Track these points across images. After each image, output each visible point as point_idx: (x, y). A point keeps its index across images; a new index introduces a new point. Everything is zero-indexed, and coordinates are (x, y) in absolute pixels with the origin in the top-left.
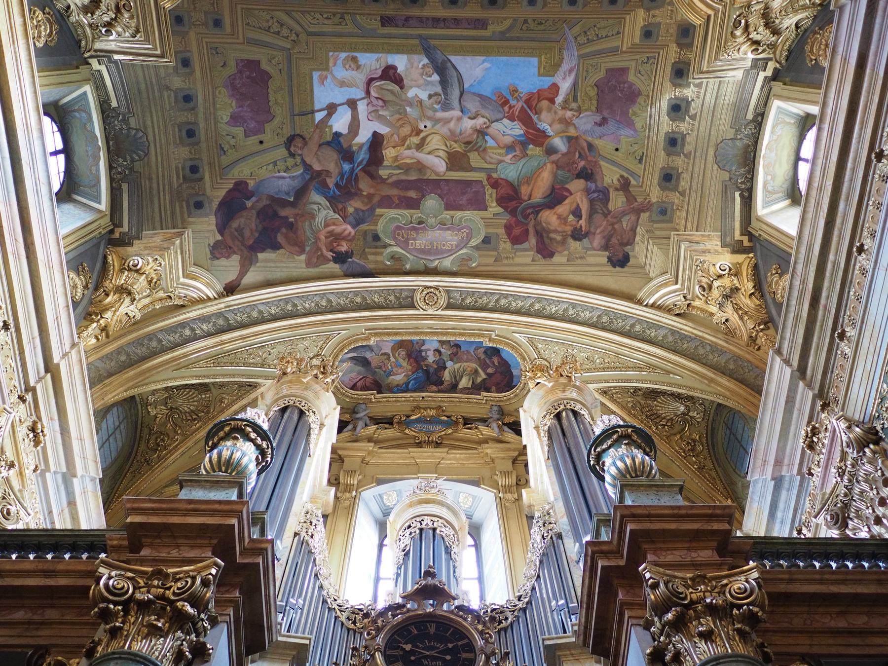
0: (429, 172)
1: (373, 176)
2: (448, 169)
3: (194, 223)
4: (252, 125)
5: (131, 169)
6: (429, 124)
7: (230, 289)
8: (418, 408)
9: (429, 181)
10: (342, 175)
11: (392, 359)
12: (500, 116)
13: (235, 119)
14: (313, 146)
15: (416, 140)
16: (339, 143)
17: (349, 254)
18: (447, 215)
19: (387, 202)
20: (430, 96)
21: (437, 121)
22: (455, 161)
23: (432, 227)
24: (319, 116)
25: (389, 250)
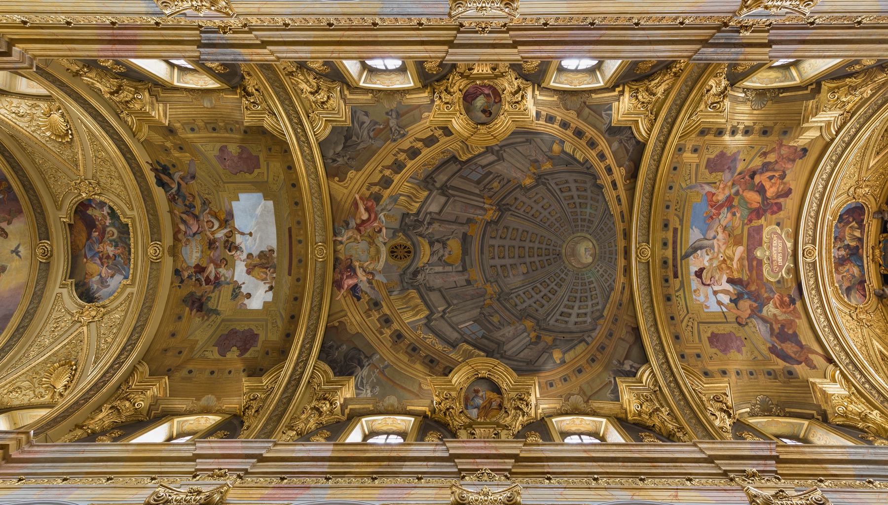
0: (744, 255)
1: (748, 284)
2: (742, 245)
3: (802, 376)
4: (739, 343)
5: (777, 405)
6: (721, 255)
7: (830, 360)
8: (873, 260)
9: (748, 255)
10: (750, 299)
11: (845, 274)
12: (717, 220)
13: (739, 351)
14: (739, 313)
15: (728, 262)
16: (735, 300)
17: (790, 296)
18: (765, 246)
20: (708, 255)
21: (719, 251)
22: (738, 242)
23: (771, 253)
24: (725, 310)
25: (784, 275)
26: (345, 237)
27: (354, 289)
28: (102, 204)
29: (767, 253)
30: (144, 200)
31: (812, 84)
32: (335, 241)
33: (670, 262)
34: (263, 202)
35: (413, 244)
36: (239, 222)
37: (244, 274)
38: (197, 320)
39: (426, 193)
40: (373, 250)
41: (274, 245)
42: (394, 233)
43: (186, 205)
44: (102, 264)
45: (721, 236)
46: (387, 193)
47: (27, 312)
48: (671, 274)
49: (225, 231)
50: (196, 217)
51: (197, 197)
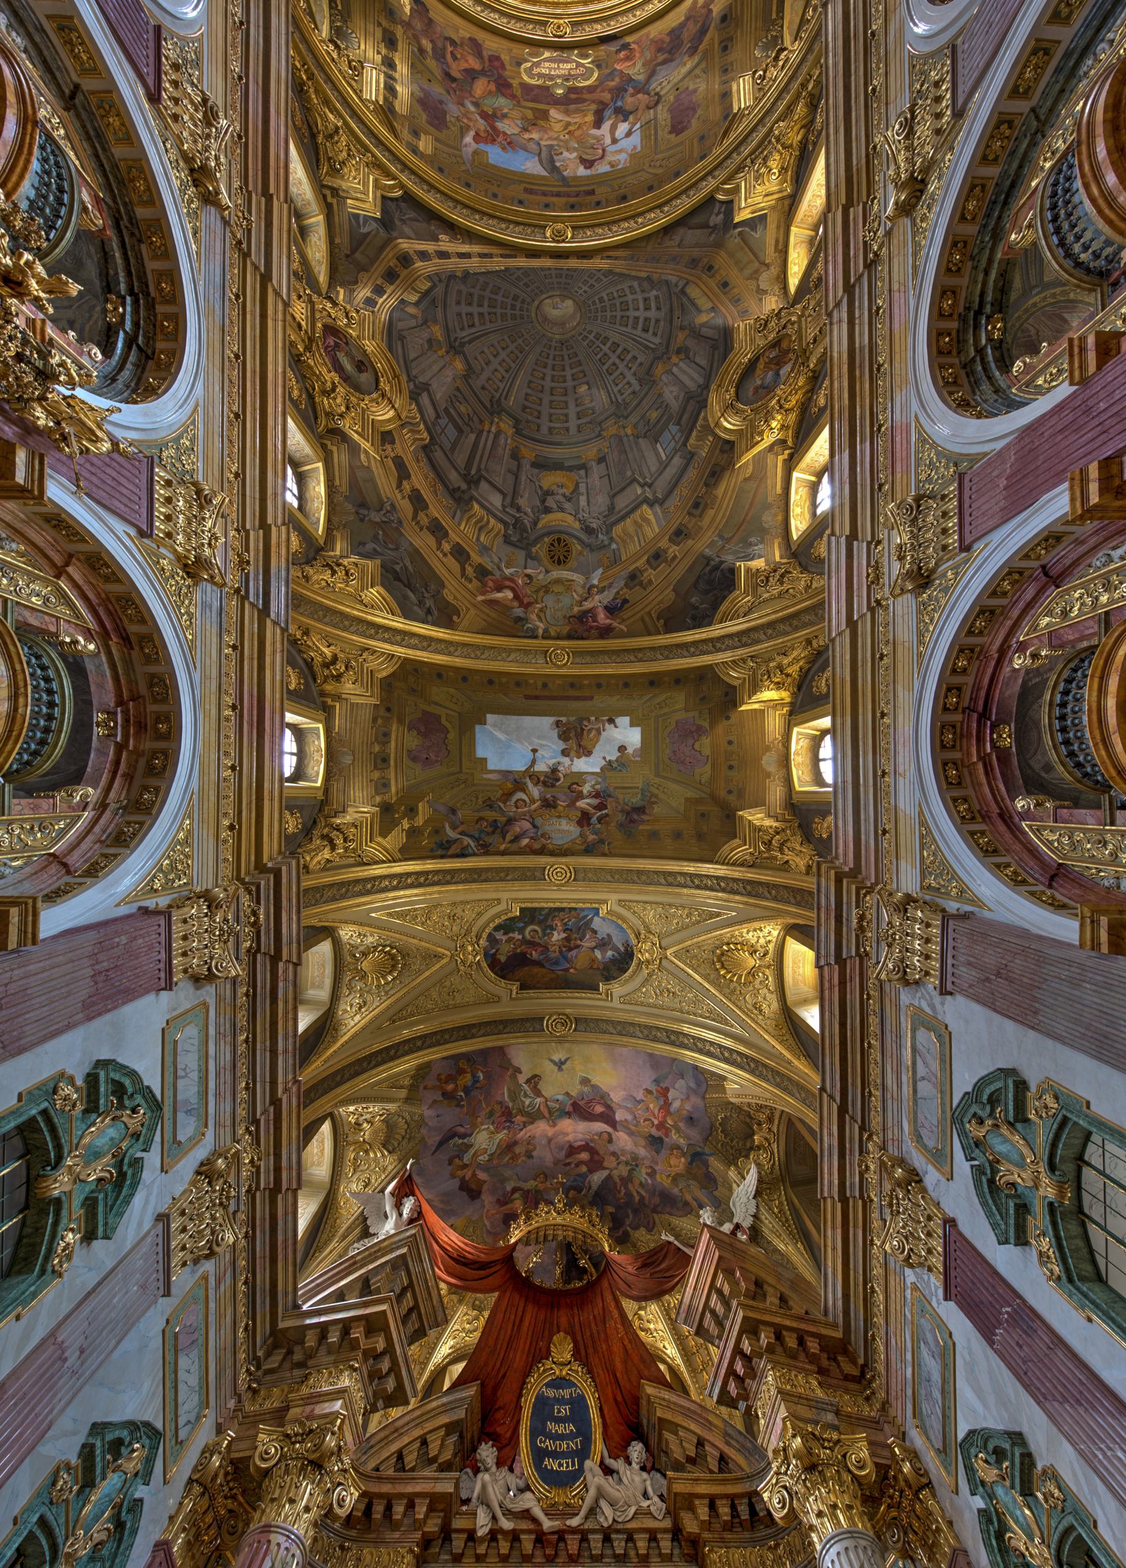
15: (571, 128)
19: (591, 89)
22: (545, 115)
23: (559, 76)
26: (538, 623)
27: (608, 609)
28: (491, 938)
29: (559, 81)
30: (485, 881)
31: (325, 197)
32: (544, 638)
33: (572, 200)
34: (487, 727)
35: (548, 534)
36: (518, 764)
37: (591, 759)
38: (656, 810)
39: (476, 506)
40: (557, 588)
41: (550, 720)
42: (532, 558)
43: (493, 833)
44: (577, 947)
45: (535, 136)
46: (476, 558)
47: (646, 1038)
48: (589, 198)
49: (530, 785)
50: (510, 821)
51: (482, 814)
